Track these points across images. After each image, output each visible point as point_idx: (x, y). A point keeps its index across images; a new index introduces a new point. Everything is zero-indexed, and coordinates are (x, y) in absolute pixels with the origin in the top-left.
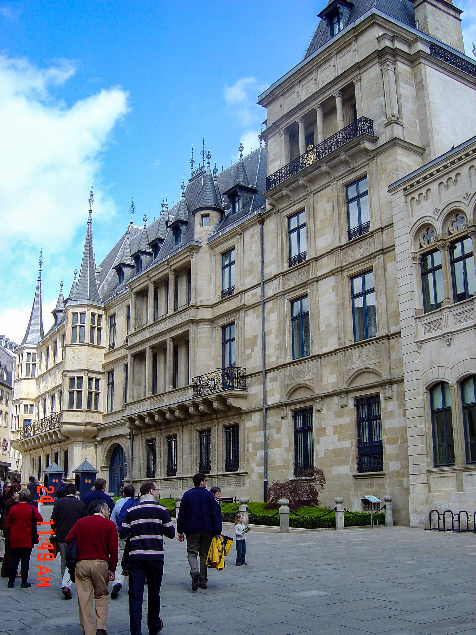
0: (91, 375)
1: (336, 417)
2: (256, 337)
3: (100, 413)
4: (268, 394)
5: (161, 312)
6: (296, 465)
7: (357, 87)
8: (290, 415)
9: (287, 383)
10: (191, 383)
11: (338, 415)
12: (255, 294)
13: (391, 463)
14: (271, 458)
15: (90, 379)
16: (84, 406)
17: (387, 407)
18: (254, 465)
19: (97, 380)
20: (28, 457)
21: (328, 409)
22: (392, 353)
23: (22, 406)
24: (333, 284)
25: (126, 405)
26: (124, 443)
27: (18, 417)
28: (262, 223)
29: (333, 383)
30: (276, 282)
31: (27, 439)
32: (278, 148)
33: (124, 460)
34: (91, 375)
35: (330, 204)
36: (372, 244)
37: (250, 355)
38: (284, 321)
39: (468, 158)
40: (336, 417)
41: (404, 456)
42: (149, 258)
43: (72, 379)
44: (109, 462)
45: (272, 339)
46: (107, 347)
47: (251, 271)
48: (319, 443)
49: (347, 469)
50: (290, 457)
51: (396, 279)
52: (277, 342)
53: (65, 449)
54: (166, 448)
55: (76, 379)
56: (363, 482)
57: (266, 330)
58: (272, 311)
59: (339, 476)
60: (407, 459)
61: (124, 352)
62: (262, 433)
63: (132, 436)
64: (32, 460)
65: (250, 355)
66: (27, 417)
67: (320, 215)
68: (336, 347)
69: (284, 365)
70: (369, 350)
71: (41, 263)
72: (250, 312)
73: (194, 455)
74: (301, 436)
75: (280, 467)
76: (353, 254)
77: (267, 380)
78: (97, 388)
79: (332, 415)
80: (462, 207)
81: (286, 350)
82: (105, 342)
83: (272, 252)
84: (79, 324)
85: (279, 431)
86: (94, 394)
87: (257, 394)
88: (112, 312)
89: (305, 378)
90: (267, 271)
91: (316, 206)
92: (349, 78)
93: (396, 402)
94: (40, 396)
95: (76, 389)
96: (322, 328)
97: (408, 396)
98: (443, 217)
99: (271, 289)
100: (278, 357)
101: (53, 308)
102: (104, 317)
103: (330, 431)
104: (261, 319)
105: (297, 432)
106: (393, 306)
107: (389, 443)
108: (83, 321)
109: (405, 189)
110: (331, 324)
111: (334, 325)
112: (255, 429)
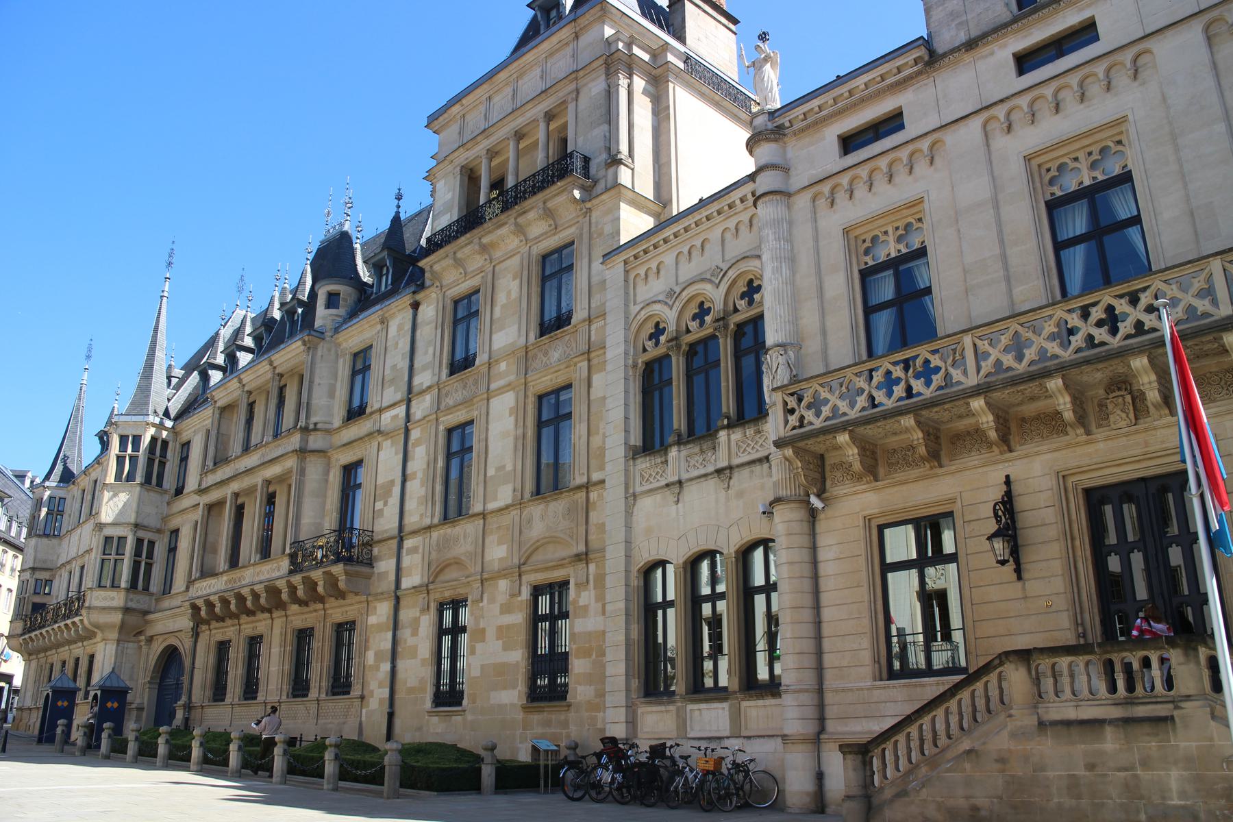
1: (502, 613)
2: (392, 482)
3: (152, 594)
4: (404, 573)
5: (254, 440)
6: (438, 684)
7: (571, 107)
8: (432, 605)
9: (434, 555)
10: (288, 551)
11: (506, 609)
12: (395, 417)
13: (580, 689)
14: (401, 675)
15: (139, 542)
17: (578, 597)
18: (373, 685)
19: (152, 544)
20: (34, 664)
21: (492, 600)
22: (591, 514)
24: (512, 403)
25: (190, 583)
26: (185, 645)
28: (416, 306)
29: (501, 559)
30: (428, 397)
31: (33, 635)
32: (449, 196)
33: (181, 672)
34: (141, 534)
35: (517, 282)
36: (574, 345)
37: (382, 510)
38: (435, 460)
39: (722, 217)
40: (502, 613)
41: (598, 677)
42: (249, 357)
43: (108, 539)
45: (415, 488)
46: (173, 491)
47: (392, 381)
48: (473, 651)
49: (513, 696)
50: (428, 673)
51: (604, 398)
52: (422, 492)
53: (89, 650)
54: (246, 653)
55: (115, 541)
56: (536, 717)
57: (409, 471)
58: (418, 443)
59: (501, 707)
60: (604, 683)
61: (195, 499)
62: (390, 634)
63: (196, 635)
65: (382, 510)
66: (38, 599)
67: (501, 298)
68: (509, 501)
69: (429, 528)
70: (558, 506)
71: (88, 357)
72: (387, 444)
73: (286, 667)
74: (447, 640)
75: (411, 690)
76: (545, 359)
77: (404, 551)
78: (150, 555)
79: (496, 608)
80: (707, 289)
81: (433, 503)
82: (169, 482)
83: (426, 353)
84: (129, 451)
85: (415, 633)
86: (143, 564)
87: (386, 573)
88: (184, 437)
89: (463, 548)
90: (417, 381)
91: (496, 283)
92: (561, 94)
93: (593, 593)
96: (491, 472)
97: (609, 581)
98: (678, 306)
99: (421, 407)
100: (421, 515)
101: (101, 427)
103: (491, 633)
104: (401, 456)
105: (441, 632)
106: (596, 441)
107: (577, 657)
108: (136, 447)
109: (626, 262)
110: (504, 467)
111: (509, 467)
112: (380, 628)
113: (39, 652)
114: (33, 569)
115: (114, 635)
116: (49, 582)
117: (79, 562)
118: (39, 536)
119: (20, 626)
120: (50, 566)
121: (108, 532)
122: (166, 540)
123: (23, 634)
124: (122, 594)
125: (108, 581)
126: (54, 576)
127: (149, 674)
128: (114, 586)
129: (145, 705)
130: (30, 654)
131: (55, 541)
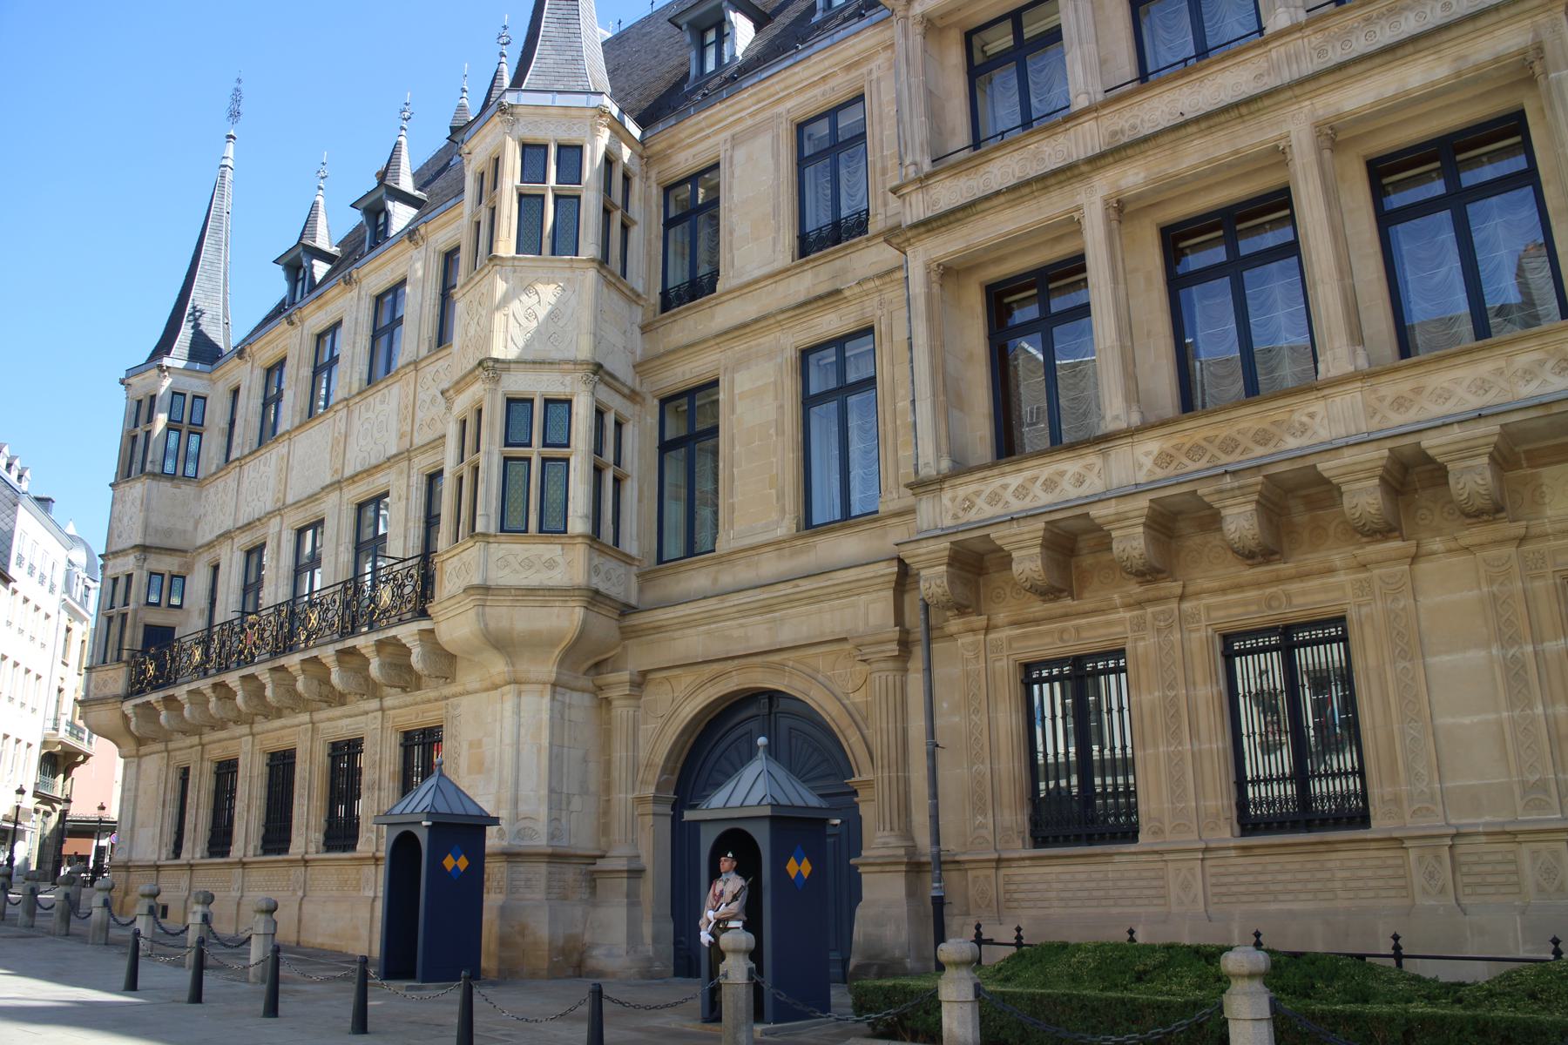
0: (605, 395)
3: (627, 559)
15: (600, 414)
16: (578, 523)
20: (154, 764)
23: (139, 579)
27: (124, 616)
43: (516, 405)
44: (675, 778)
46: (655, 298)
64: (174, 778)
66: (158, 618)
71: (235, 115)
94: (226, 535)
95: (535, 452)
102: (636, 184)
113: (166, 737)
114: (144, 549)
115: (547, 669)
116: (179, 579)
117: (245, 540)
118: (153, 475)
119: (116, 679)
120: (176, 542)
121: (518, 383)
122: (652, 420)
123: (128, 696)
124: (580, 552)
125: (529, 510)
126: (190, 567)
127: (653, 776)
128: (553, 526)
129: (646, 860)
130: (140, 741)
131: (188, 489)
